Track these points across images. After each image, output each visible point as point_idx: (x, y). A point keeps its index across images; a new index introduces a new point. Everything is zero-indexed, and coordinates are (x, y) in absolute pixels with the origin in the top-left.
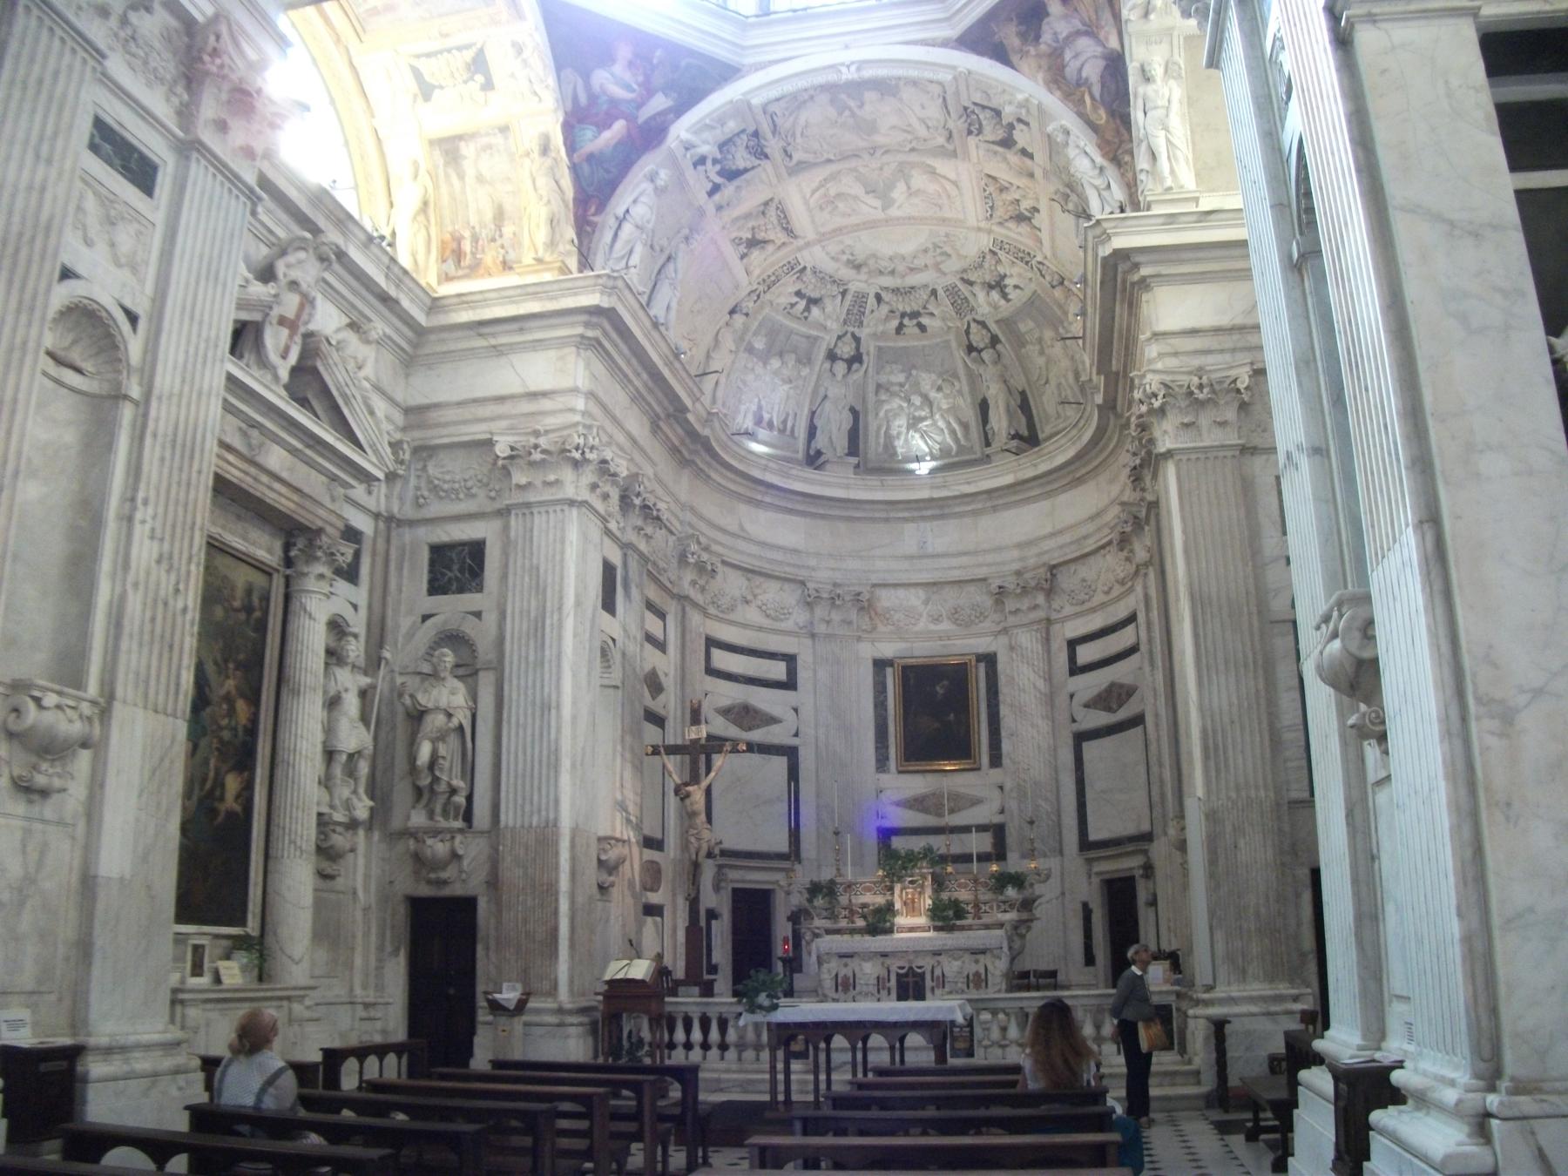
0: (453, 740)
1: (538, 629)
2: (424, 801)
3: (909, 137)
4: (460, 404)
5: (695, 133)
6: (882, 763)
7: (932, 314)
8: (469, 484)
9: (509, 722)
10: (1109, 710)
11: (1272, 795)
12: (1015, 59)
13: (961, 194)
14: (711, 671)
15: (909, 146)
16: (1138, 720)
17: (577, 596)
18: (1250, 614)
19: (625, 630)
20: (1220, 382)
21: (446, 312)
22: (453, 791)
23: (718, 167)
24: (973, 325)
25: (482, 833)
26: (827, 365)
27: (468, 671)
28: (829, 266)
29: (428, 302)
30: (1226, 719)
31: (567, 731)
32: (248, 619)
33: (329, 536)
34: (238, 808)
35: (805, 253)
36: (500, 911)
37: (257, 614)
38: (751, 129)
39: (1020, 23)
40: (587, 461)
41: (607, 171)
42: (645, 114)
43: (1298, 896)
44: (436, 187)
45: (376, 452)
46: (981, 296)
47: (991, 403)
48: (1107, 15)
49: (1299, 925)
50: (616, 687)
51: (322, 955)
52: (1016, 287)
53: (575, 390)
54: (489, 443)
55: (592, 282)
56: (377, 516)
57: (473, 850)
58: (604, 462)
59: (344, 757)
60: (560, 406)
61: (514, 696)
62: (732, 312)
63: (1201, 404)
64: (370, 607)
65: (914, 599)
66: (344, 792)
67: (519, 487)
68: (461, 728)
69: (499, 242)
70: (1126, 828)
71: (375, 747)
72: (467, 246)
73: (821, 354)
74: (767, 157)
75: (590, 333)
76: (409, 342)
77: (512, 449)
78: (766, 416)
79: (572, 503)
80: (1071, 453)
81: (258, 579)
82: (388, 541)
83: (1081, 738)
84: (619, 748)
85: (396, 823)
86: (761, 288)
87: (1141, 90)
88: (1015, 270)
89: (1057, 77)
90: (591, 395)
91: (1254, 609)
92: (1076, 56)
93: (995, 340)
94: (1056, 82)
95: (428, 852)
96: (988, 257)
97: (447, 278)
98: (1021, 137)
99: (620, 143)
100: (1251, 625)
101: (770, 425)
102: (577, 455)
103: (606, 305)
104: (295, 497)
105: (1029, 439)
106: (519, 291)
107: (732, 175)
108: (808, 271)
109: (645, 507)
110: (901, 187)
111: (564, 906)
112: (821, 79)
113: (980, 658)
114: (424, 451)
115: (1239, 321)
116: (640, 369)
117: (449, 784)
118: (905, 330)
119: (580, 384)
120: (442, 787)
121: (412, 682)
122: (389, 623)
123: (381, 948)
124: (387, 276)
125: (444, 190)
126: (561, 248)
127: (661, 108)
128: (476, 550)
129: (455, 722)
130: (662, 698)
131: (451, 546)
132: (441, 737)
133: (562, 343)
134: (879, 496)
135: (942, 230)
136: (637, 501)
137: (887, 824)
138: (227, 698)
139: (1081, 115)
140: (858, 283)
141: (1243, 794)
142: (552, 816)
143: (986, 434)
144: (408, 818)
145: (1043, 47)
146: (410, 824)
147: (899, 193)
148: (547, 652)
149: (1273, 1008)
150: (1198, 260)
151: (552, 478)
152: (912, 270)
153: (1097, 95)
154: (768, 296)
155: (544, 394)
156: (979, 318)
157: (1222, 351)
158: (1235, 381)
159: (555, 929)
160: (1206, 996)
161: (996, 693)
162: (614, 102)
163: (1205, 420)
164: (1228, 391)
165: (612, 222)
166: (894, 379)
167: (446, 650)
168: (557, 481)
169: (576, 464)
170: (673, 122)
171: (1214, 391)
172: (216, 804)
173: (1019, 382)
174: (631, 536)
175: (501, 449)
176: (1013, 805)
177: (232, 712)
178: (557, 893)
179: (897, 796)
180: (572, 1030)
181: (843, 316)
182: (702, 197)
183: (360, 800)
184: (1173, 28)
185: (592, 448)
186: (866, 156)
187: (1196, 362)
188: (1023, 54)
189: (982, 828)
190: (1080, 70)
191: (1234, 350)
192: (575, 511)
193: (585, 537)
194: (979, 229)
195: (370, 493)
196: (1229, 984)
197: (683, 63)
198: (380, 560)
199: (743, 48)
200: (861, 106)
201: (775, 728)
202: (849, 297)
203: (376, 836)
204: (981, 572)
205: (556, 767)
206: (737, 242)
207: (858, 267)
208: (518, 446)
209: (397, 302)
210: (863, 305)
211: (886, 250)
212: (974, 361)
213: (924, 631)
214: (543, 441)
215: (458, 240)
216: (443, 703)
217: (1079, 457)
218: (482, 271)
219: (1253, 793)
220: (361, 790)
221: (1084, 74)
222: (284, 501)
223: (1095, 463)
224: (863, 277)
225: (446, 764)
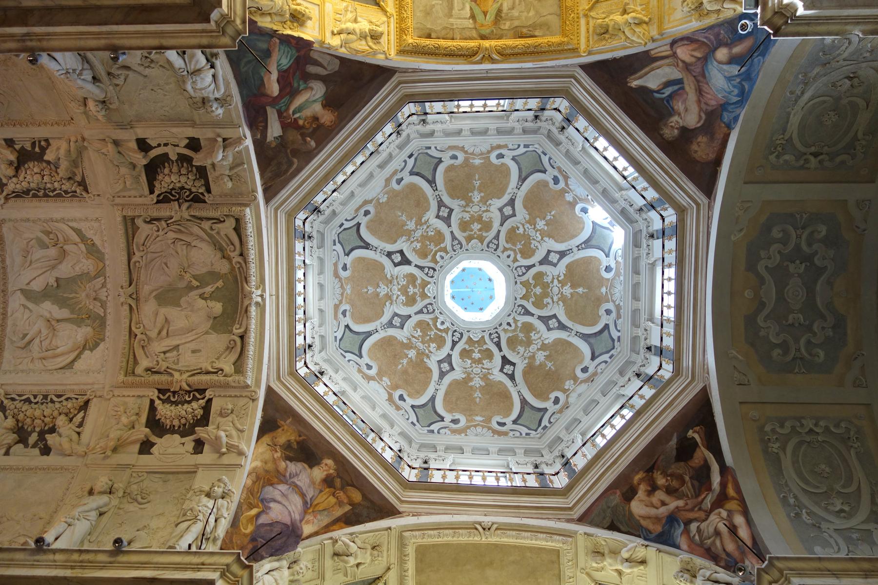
3: (153, 334)
5: (239, 152)
12: (266, 439)
23: (173, 157)
38: (207, 197)
39: (298, 443)
42: (272, 115)
48: (326, 520)
74: (158, 202)
94: (258, 478)
99: (262, 84)
103: (215, 15)
107: (152, 170)
110: (65, 313)
112: (253, 269)
145: (283, 464)
147: (48, 308)
153: (261, 521)
170: (253, 136)
182: (141, 133)
186: (131, 289)
188: (273, 446)
190: (275, 501)
197: (295, 160)
199: (276, 210)
200: (201, 296)
221: (272, 505)
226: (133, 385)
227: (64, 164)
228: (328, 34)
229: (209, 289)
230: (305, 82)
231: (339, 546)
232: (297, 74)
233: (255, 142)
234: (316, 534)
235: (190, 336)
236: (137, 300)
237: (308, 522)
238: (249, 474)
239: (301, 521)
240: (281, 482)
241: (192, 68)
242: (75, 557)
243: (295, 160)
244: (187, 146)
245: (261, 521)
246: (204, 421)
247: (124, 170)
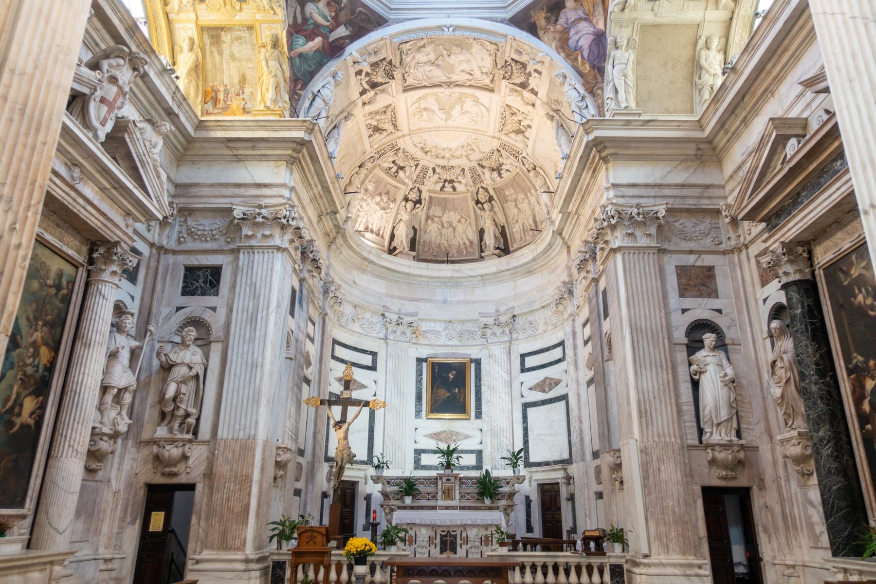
0: (192, 384)
1: (253, 319)
2: (166, 422)
4: (212, 185)
6: (418, 413)
7: (460, 182)
8: (215, 232)
9: (230, 374)
10: (544, 391)
11: (679, 441)
12: (541, 33)
13: (489, 116)
14: (334, 357)
15: (469, 83)
16: (564, 397)
17: (278, 302)
18: (663, 338)
19: (299, 327)
20: (648, 213)
21: (207, 130)
22: (188, 415)
23: (367, 79)
24: (481, 190)
25: (204, 442)
26: (404, 203)
27: (204, 342)
28: (412, 150)
29: (197, 122)
30: (651, 396)
31: (266, 380)
32: (57, 294)
33: (122, 248)
34: (31, 422)
35: (401, 139)
36: (212, 493)
37: (65, 291)
38: (388, 60)
39: (547, 12)
40: (290, 226)
41: (309, 66)
42: (334, 36)
43: (695, 502)
44: (204, 57)
45: (158, 201)
46: (487, 173)
47: (486, 231)
48: (600, 9)
49: (697, 520)
50: (291, 359)
51: (80, 525)
52: (507, 170)
53: (284, 185)
54: (230, 210)
55: (300, 124)
56: (152, 245)
57: (198, 454)
58: (298, 228)
59: (116, 391)
60: (275, 193)
61: (235, 358)
62: (360, 167)
63: (639, 224)
64: (142, 299)
65: (439, 327)
66: (112, 414)
67: (247, 236)
68: (197, 376)
69: (241, 97)
70: (556, 457)
71: (138, 384)
72: (221, 96)
73: (400, 197)
75: (295, 155)
76: (182, 145)
77: (244, 214)
78: (370, 227)
79: (279, 249)
80: (531, 257)
81: (68, 269)
82: (158, 261)
83: (526, 406)
84: (290, 394)
85: (146, 435)
86: (377, 156)
87: (613, 53)
88: (509, 161)
89: (564, 46)
90: (292, 189)
91: (666, 336)
92: (577, 33)
93: (491, 199)
94: (562, 47)
95: (167, 454)
96: (495, 153)
97: (208, 113)
98: (533, 82)
99: (317, 50)
100: (664, 344)
101: (372, 231)
102: (284, 221)
103: (307, 138)
104: (101, 218)
105: (505, 250)
106: (255, 124)
107: (374, 85)
108: (401, 151)
109: (314, 260)
110: (458, 108)
111: (255, 490)
113: (472, 361)
114: (185, 212)
115: (658, 181)
116: (318, 183)
117: (186, 410)
118: (445, 189)
119: (287, 181)
120: (181, 412)
121: (168, 348)
122: (154, 310)
123: (122, 520)
124: (173, 98)
125: (209, 60)
126: (280, 104)
127: (343, 35)
128: (216, 271)
129: (194, 372)
130: (311, 369)
131: (199, 268)
132: (184, 382)
133: (278, 159)
134: (425, 273)
135: (474, 136)
136: (311, 256)
137: (420, 446)
138: (34, 344)
139: (575, 68)
140: (427, 161)
141: (662, 439)
142: (252, 433)
143: (481, 246)
144: (155, 432)
145: (558, 27)
146: (155, 436)
147: (456, 112)
148: (258, 333)
149: (689, 572)
150: (638, 148)
151: (268, 233)
152: (453, 157)
153: (586, 57)
154: (379, 162)
155: (266, 186)
156: (484, 186)
157: (649, 197)
158: (656, 213)
159: (248, 505)
160: (645, 561)
161: (480, 380)
162: (317, 25)
163: (638, 233)
164: (652, 218)
165: (310, 96)
166: (436, 214)
167: (192, 328)
168: (271, 235)
169: (283, 227)
171: (644, 217)
172: (13, 418)
173: (502, 220)
174: (306, 275)
175: (238, 213)
176: (487, 440)
177: (36, 354)
178: (251, 481)
179: (425, 433)
180: (253, 574)
181: (415, 178)
183: (122, 419)
184: (635, 19)
185: (293, 219)
187: (635, 201)
188: (546, 30)
189: (471, 452)
190: (578, 41)
191: (655, 197)
192: (280, 255)
193: (284, 269)
194: (494, 137)
195: (149, 231)
196: (659, 554)
197: (358, 10)
198: (151, 271)
199: (391, 9)
200: (449, 55)
201: (364, 391)
202: (419, 168)
203: (130, 443)
204: (476, 316)
205: (257, 402)
206: (369, 126)
207: (426, 153)
208: (248, 213)
209: (177, 116)
210: (425, 173)
211: (444, 144)
212: (479, 208)
213: (445, 347)
214: (264, 212)
215: (216, 92)
216: (187, 361)
217: (534, 260)
218: (230, 112)
219: (667, 439)
220: (124, 413)
221: (580, 44)
222: (94, 220)
223: (542, 263)
224: (428, 157)
225: (186, 398)
226: (500, 90)
227: (378, 117)
228: (277, 18)
229: (445, 52)
230: (308, 20)
231: (617, 9)
232: (305, 28)
233: (352, 41)
234: (606, 19)
235: (473, 60)
236: (451, 83)
237: (597, 23)
238: (558, 53)
239: (595, 28)
240: (568, 32)
241: (323, 105)
242: (566, 170)
243: (358, 10)
244: (360, 74)
245: (586, 57)
246: (524, 66)
247: (378, 97)
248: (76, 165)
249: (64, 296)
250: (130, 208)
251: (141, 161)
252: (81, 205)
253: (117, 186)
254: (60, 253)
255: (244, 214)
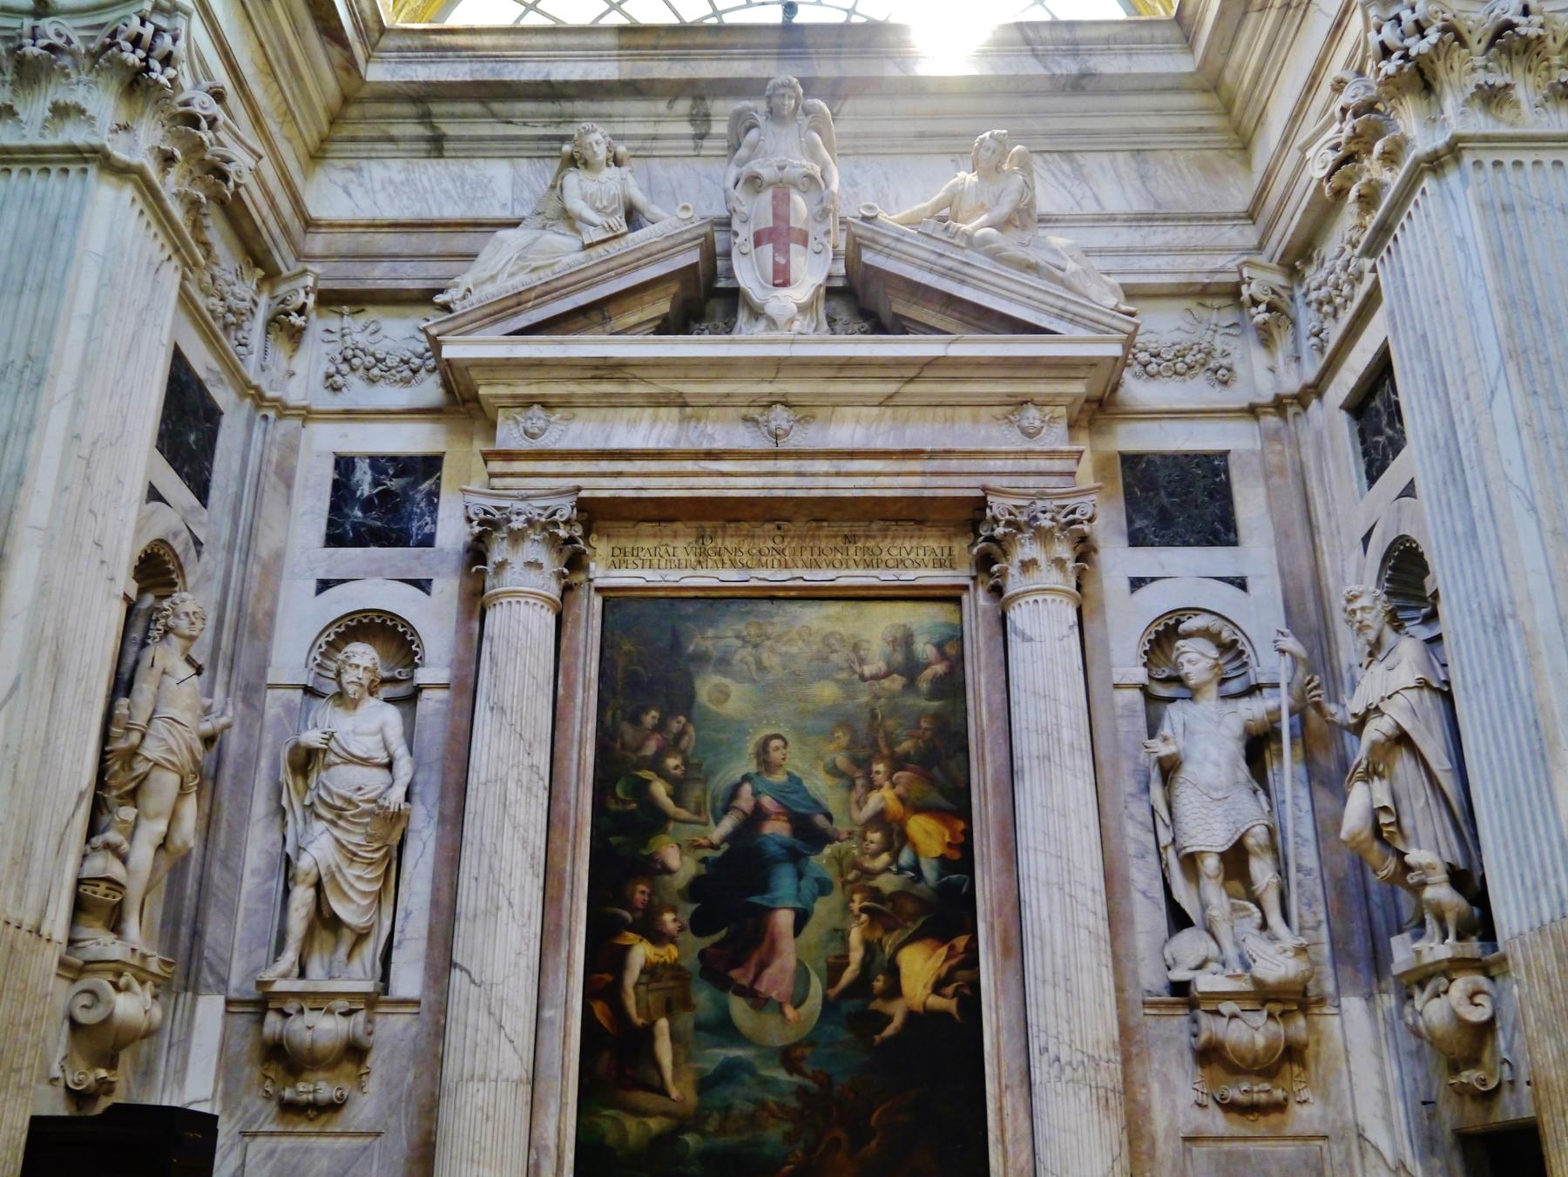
29: (1174, 32)
77: (1335, 148)
81: (924, 619)
192: (1453, 177)
248: (769, 406)
249: (937, 681)
250: (1003, 388)
251: (946, 273)
252: (827, 474)
253: (912, 373)
254: (872, 593)
255: (1335, 148)
